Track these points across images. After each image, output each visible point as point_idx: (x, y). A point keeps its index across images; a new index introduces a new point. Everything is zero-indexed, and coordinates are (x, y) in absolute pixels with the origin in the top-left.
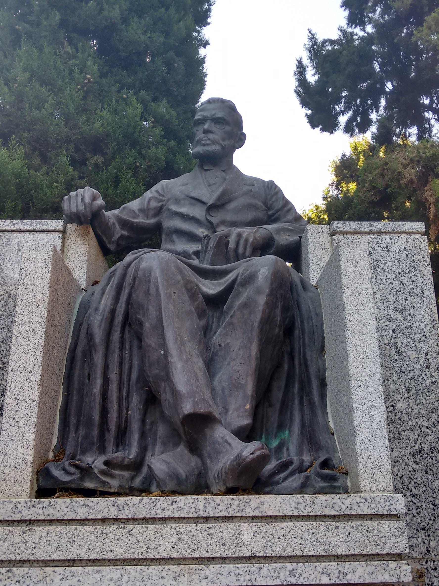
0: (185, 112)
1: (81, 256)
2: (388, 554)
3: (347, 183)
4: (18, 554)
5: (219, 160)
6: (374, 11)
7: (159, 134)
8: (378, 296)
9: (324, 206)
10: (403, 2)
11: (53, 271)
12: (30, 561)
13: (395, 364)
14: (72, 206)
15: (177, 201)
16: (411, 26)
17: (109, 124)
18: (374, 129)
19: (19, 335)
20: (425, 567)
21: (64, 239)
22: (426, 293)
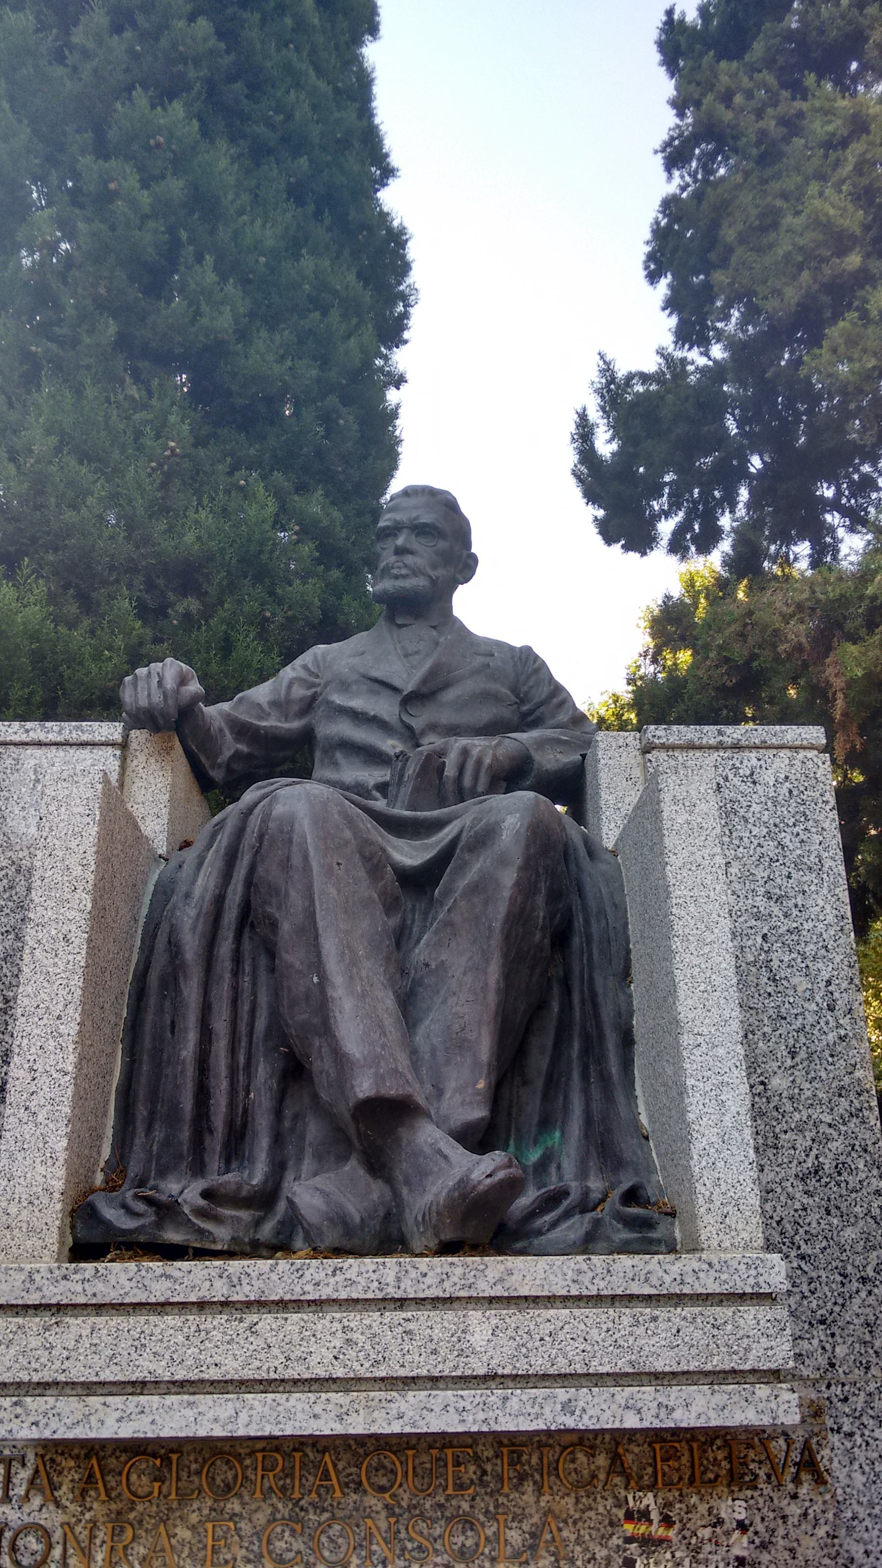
0: (359, 514)
1: (157, 794)
2: (753, 1371)
3: (674, 651)
4: (35, 1370)
5: (425, 606)
6: (727, 318)
7: (309, 557)
8: (733, 870)
9: (630, 696)
10: (782, 300)
11: (103, 822)
12: (58, 1383)
13: (766, 1001)
14: (139, 696)
15: (344, 686)
16: (799, 346)
17: (211, 537)
18: (725, 546)
19: (36, 946)
20: (826, 1396)
21: (124, 759)
22: (828, 863)
